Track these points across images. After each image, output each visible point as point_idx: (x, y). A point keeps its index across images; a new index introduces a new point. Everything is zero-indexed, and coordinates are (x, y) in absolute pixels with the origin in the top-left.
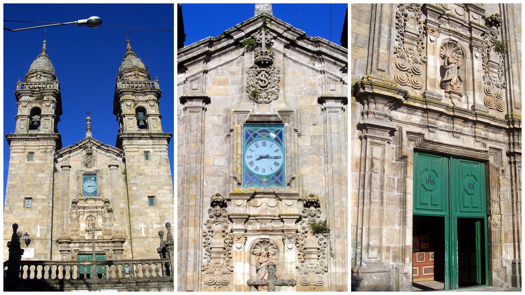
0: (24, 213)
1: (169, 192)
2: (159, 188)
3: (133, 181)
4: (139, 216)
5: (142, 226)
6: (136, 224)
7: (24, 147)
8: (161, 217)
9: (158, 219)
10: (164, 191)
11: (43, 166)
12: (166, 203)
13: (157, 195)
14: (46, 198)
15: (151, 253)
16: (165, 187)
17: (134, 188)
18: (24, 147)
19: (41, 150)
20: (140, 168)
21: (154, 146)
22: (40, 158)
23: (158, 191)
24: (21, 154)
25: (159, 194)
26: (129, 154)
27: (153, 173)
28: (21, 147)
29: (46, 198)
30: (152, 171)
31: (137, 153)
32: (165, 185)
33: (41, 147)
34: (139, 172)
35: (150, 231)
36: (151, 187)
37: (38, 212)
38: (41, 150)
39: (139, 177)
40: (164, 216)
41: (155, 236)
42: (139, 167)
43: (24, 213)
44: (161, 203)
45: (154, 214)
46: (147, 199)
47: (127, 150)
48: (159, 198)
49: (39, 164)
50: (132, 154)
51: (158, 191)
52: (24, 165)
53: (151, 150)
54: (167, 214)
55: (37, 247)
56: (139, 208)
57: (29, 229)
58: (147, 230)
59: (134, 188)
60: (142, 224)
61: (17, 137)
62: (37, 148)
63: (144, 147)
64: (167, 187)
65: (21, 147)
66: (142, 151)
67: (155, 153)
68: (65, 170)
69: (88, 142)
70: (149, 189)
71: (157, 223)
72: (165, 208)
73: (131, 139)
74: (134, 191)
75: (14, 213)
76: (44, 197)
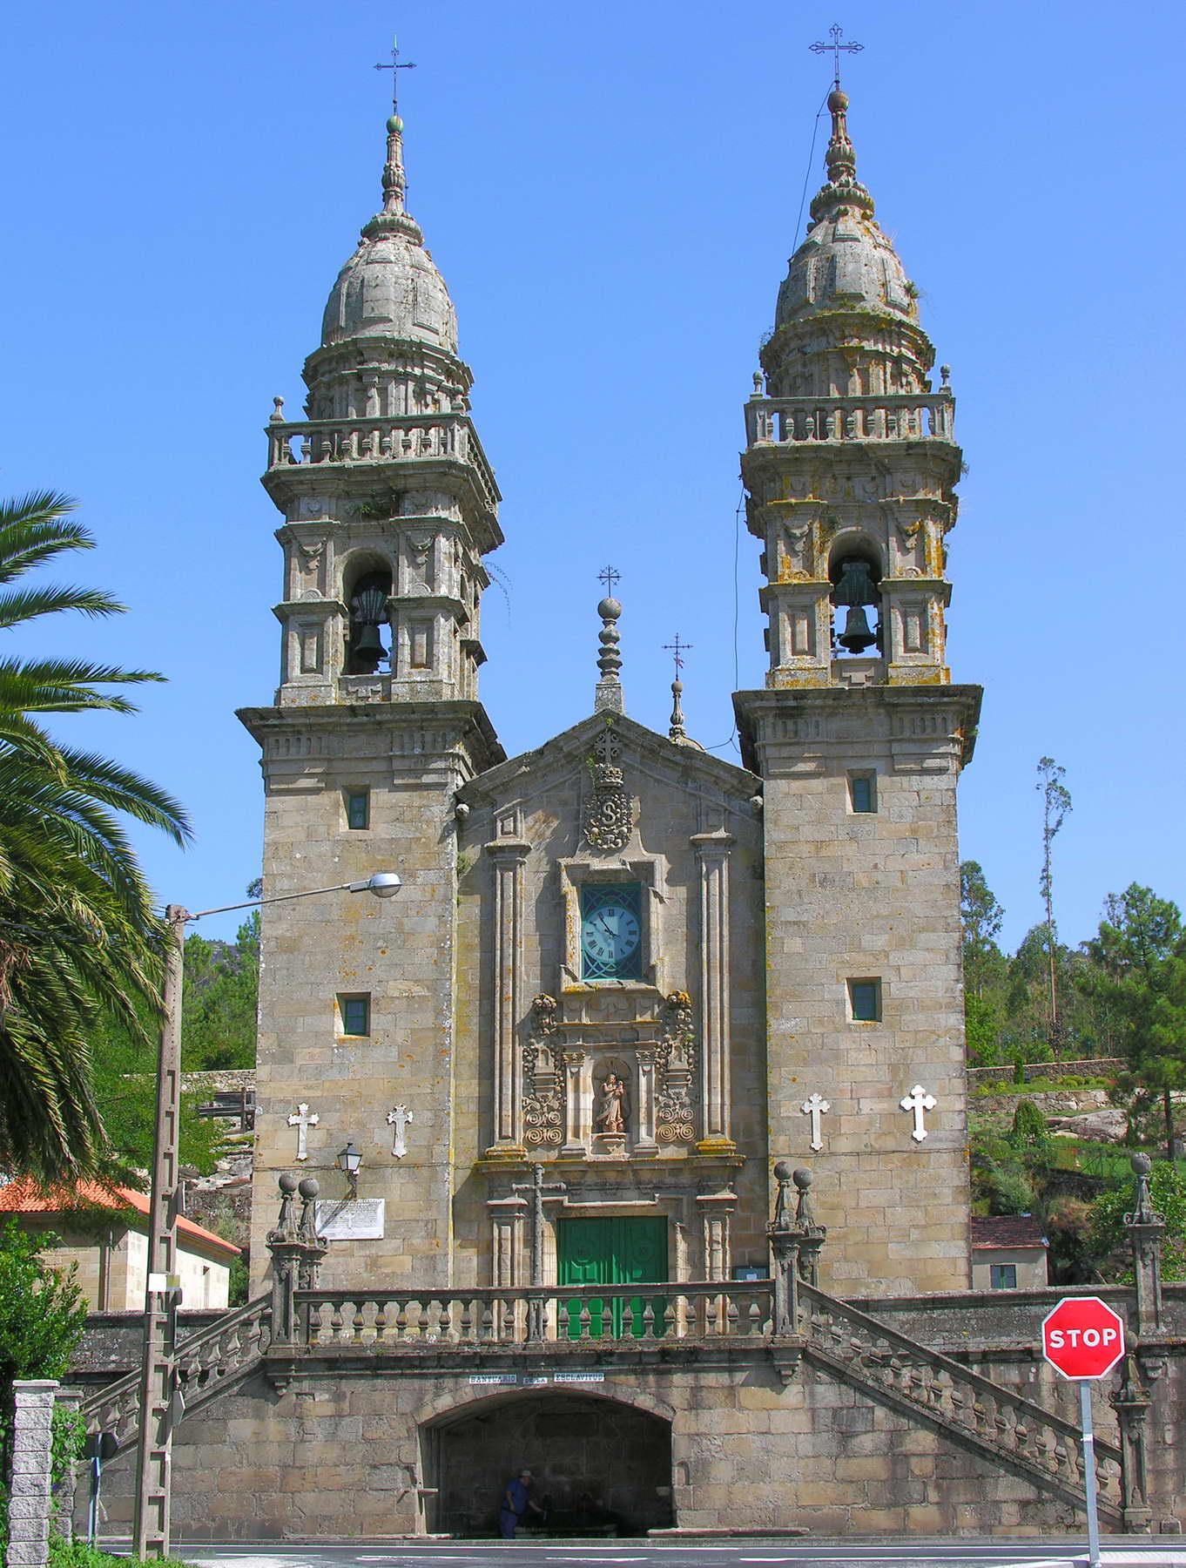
0: (338, 1061)
2: (903, 943)
3: (789, 915)
4: (805, 1062)
5: (817, 1105)
6: (791, 1097)
8: (894, 1068)
10: (920, 956)
11: (409, 850)
12: (924, 1008)
13: (887, 976)
14: (425, 993)
15: (841, 1214)
16: (923, 936)
17: (794, 944)
20: (823, 853)
23: (894, 958)
26: (782, 783)
27: (879, 876)
29: (425, 993)
30: (876, 866)
32: (923, 930)
36: (867, 940)
37: (394, 1052)
43: (338, 1061)
44: (902, 1007)
45: (866, 1058)
48: (893, 990)
50: (796, 785)
52: (326, 848)
54: (920, 1056)
55: (396, 1194)
57: (361, 1125)
58: (832, 1122)
59: (794, 944)
60: (816, 1098)
64: (933, 936)
71: (879, 1096)
72: (917, 1032)
73: (792, 716)
75: (299, 1062)
76: (419, 991)
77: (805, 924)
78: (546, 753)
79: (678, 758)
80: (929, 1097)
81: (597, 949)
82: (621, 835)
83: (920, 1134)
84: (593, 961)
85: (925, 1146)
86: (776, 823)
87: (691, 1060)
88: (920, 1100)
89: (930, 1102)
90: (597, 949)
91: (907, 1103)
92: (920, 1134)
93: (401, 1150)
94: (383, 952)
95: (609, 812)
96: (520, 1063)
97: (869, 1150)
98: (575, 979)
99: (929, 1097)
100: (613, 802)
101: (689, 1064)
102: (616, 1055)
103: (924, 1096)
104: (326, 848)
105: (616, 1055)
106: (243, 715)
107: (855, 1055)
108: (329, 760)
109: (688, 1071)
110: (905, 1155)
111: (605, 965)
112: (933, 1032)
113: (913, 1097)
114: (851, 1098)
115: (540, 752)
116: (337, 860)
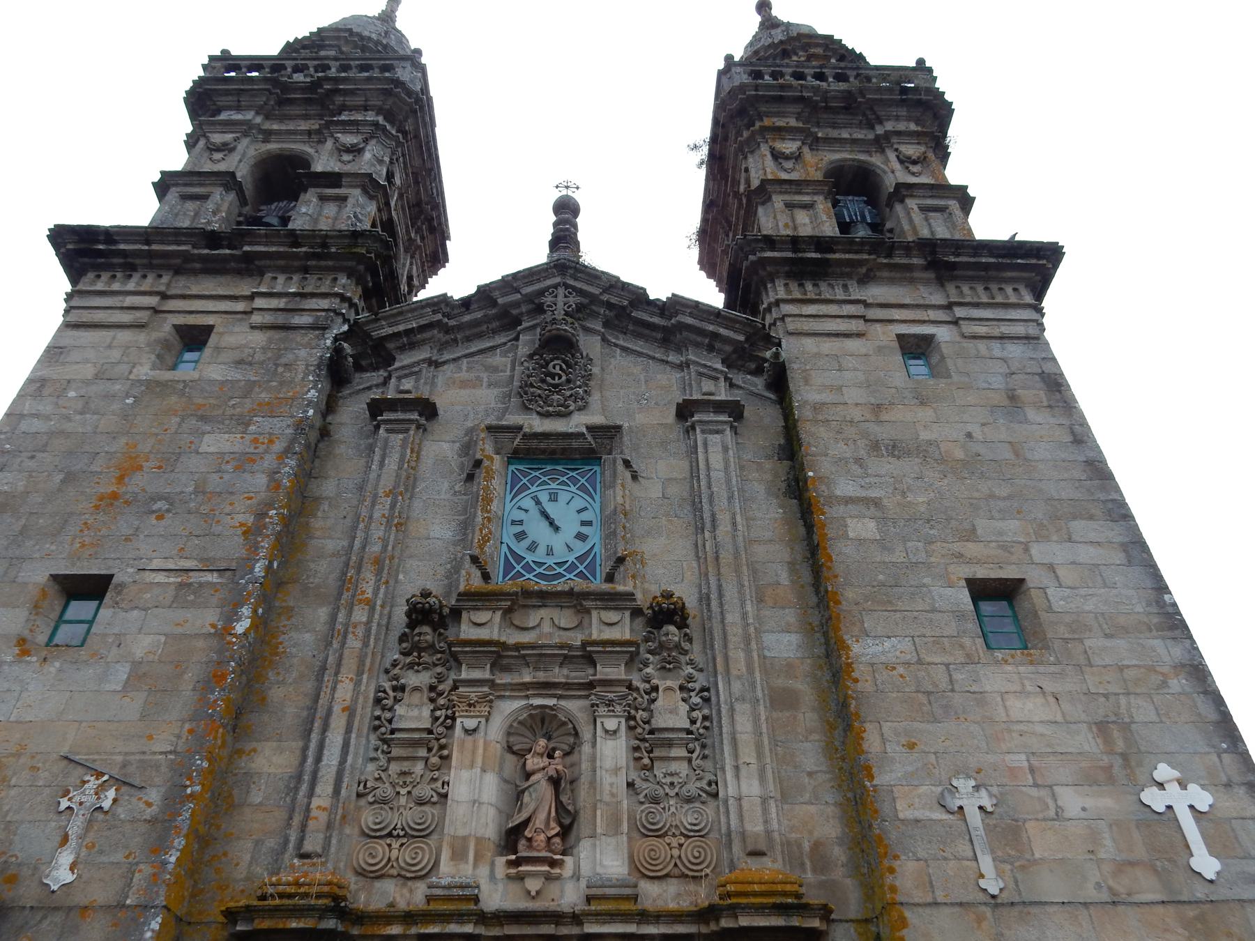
2: (1041, 535)
7: (152, 301)
8: (1102, 728)
9: (1086, 742)
13: (1034, 577)
16: (1079, 527)
17: (862, 527)
18: (152, 301)
19: (257, 319)
20: (884, 417)
21: (960, 312)
23: (1038, 552)
24: (124, 336)
28: (130, 301)
30: (969, 435)
31: (852, 345)
33: (260, 303)
34: (883, 433)
35: (1042, 844)
36: (982, 525)
38: (257, 319)
39: (886, 466)
40: (1126, 727)
41: (1091, 893)
42: (877, 408)
46: (965, 597)
47: (791, 325)
49: (223, 383)
50: (828, 346)
51: (1035, 550)
53: (943, 334)
56: (920, 662)
61: (122, 247)
62: (240, 306)
63: (896, 314)
65: (130, 301)
66: (885, 335)
67: (969, 345)
68: (399, 427)
69: (556, 286)
70: (970, 535)
74: (861, 541)
77: (876, 503)
78: (474, 306)
79: (656, 320)
80: (1193, 787)
81: (525, 543)
82: (575, 397)
84: (519, 559)
85: (1222, 893)
86: (807, 381)
87: (695, 714)
90: (525, 543)
92: (1206, 863)
93: (61, 874)
94: (160, 518)
95: (557, 370)
96: (366, 711)
97: (1105, 896)
98: (486, 577)
99: (1193, 787)
100: (564, 361)
101: (693, 722)
102: (551, 702)
103: (1183, 785)
105: (551, 702)
107: (1018, 704)
108: (164, 296)
109: (689, 732)
110: (1191, 912)
111: (540, 564)
112: (1151, 669)
113: (1161, 786)
114: (1036, 785)
115: (466, 303)
116: (130, 401)
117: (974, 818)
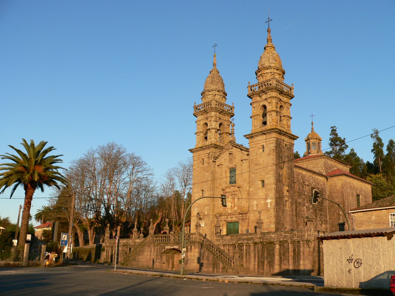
1: (272, 176)
5: (255, 202)
8: (266, 195)
10: (270, 176)
16: (270, 172)
22: (206, 162)
23: (266, 176)
25: (266, 178)
30: (264, 161)
42: (256, 159)
44: (267, 185)
48: (266, 182)
51: (266, 176)
58: (257, 205)
63: (260, 142)
64: (271, 172)
83: (269, 206)
88: (269, 201)
89: (270, 201)
91: (267, 201)
104: (199, 168)
106: (189, 150)
117: (255, 204)
